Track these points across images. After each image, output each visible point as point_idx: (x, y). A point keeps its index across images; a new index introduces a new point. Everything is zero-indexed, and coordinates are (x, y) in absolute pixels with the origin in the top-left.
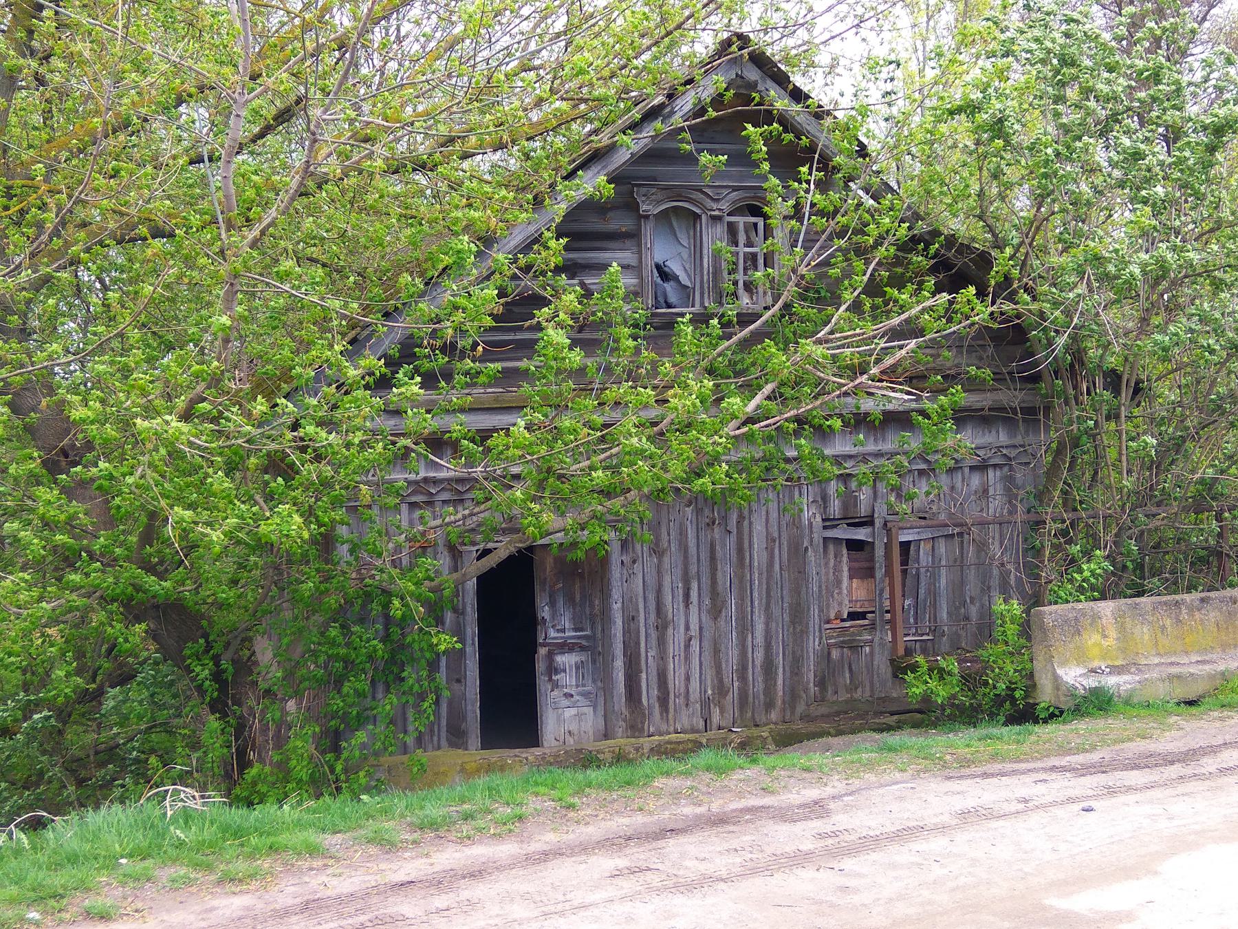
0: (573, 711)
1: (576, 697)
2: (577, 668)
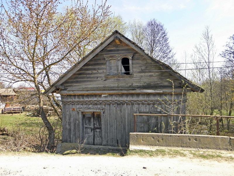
0: (99, 139)
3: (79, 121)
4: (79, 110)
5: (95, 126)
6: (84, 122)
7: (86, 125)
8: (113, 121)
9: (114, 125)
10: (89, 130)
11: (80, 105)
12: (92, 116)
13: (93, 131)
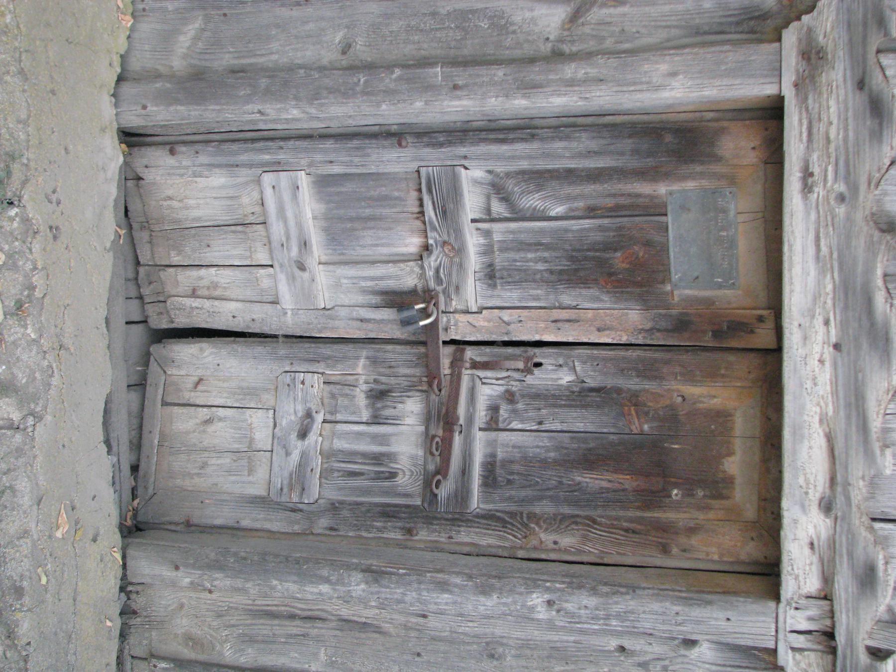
0: (262, 437)
2: (377, 459)
3: (558, 56)
4: (813, 56)
6: (563, 154)
7: (497, 188)
10: (397, 249)
12: (681, 324)
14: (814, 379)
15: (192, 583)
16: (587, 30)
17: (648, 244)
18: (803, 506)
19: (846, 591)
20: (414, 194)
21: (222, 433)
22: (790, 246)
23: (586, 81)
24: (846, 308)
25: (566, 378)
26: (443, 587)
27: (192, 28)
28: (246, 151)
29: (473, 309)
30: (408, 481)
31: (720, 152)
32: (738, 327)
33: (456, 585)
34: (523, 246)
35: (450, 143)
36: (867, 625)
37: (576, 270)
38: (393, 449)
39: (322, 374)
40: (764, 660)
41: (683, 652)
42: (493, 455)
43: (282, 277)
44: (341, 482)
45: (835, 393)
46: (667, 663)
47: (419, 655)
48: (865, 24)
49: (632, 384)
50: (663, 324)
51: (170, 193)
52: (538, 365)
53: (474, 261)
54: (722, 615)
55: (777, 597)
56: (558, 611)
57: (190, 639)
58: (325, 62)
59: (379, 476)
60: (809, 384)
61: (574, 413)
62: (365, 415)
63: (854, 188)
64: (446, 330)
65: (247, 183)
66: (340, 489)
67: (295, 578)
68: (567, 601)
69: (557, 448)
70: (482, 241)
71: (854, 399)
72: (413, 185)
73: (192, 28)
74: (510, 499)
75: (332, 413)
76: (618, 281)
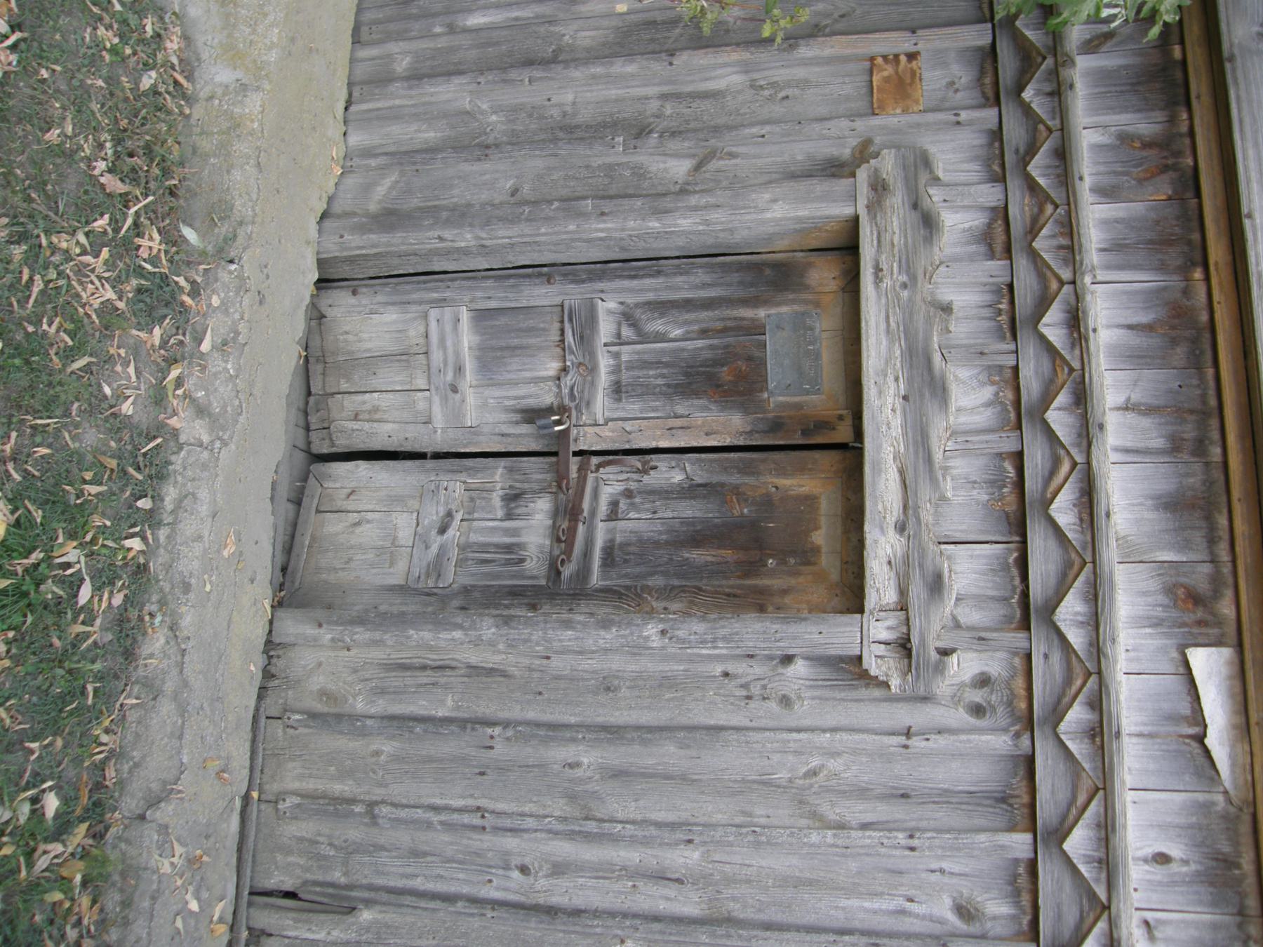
0: (405, 535)
1: (436, 542)
2: (509, 548)
3: (683, 192)
4: (879, 187)
5: (608, 472)
6: (683, 286)
7: (627, 316)
8: (685, 858)
9: (603, 871)
11: (990, 195)
12: (776, 426)
13: (525, 437)
14: (888, 424)
15: (333, 640)
16: (707, 175)
17: (750, 359)
18: (882, 529)
19: (919, 598)
20: (557, 325)
21: (369, 534)
22: (867, 322)
23: (706, 207)
24: (911, 366)
25: (678, 477)
26: (568, 624)
27: (388, 182)
28: (418, 290)
29: (602, 421)
30: (535, 565)
31: (808, 282)
32: (823, 425)
33: (579, 622)
34: (645, 365)
35: (590, 280)
36: (936, 627)
37: (690, 383)
38: (523, 539)
39: (464, 482)
40: (850, 672)
41: (780, 670)
42: (612, 541)
43: (436, 399)
44: (473, 569)
45: (905, 434)
46: (766, 682)
47: (540, 693)
48: (916, 166)
49: (734, 479)
50: (761, 426)
51: (347, 328)
52: (655, 468)
53: (604, 378)
54: (814, 629)
55: (861, 610)
56: (671, 638)
57: (324, 694)
58: (497, 202)
59: (508, 563)
60: (884, 428)
61: (684, 503)
62: (500, 513)
63: (913, 278)
64: (576, 440)
65: (415, 319)
66: (473, 575)
67: (430, 627)
68: (679, 629)
69: (668, 532)
70: (612, 362)
71: (919, 437)
72: (556, 318)
73: (388, 182)
74: (626, 576)
75: (469, 513)
76: (725, 391)
